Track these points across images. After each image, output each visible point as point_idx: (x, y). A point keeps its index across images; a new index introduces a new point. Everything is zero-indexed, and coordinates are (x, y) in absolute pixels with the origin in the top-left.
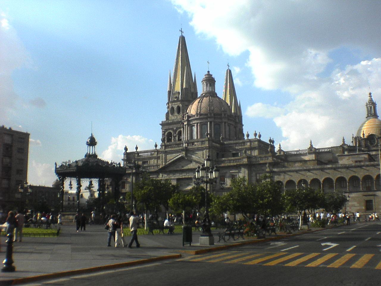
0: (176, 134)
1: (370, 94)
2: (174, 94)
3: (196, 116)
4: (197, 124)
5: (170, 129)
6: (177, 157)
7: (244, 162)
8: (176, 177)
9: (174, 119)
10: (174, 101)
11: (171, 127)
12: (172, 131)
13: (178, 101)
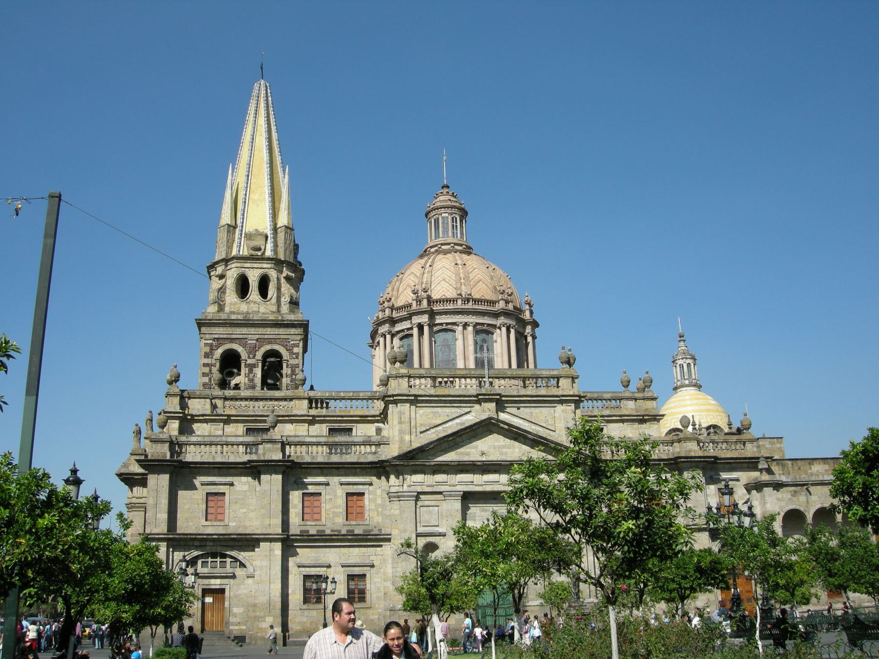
0: (254, 357)
2: (249, 236)
3: (460, 302)
4: (465, 325)
5: (232, 340)
6: (458, 421)
7: (690, 451)
8: (459, 488)
9: (248, 313)
10: (251, 258)
11: (238, 332)
13: (262, 259)
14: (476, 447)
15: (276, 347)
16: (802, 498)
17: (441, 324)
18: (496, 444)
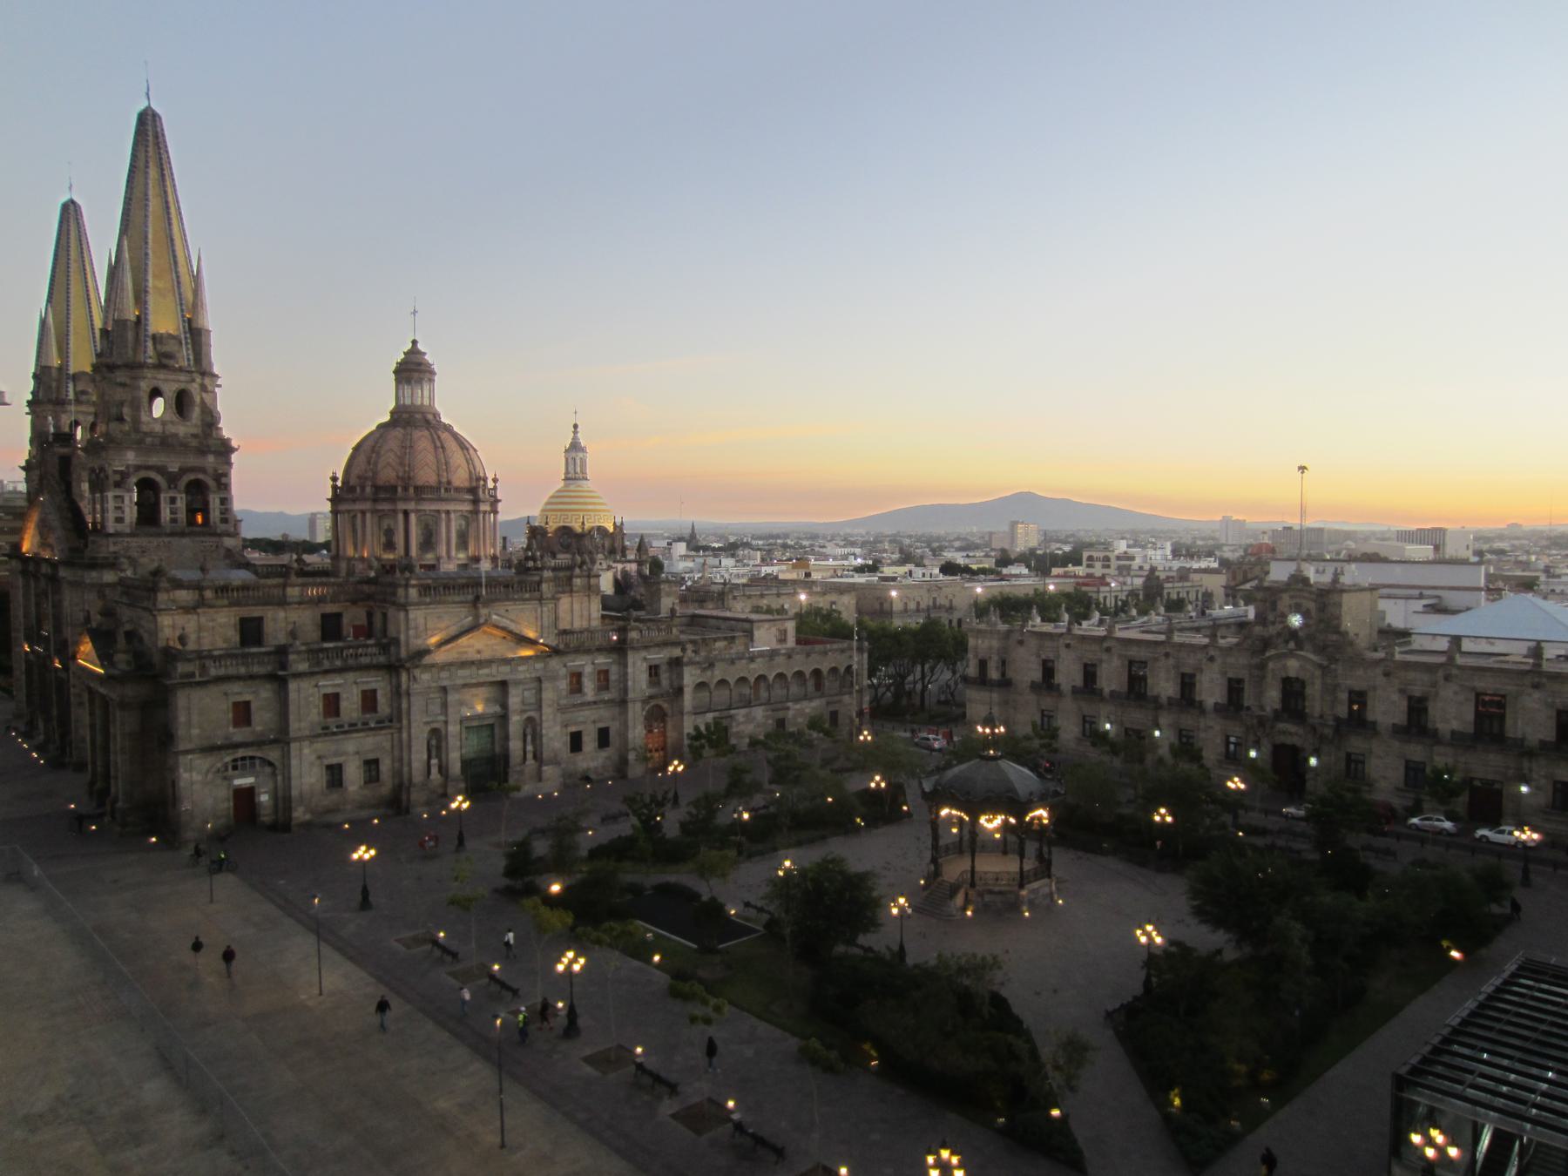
1: (576, 426)
4: (448, 512)
12: (158, 478)
15: (201, 476)
16: (709, 673)
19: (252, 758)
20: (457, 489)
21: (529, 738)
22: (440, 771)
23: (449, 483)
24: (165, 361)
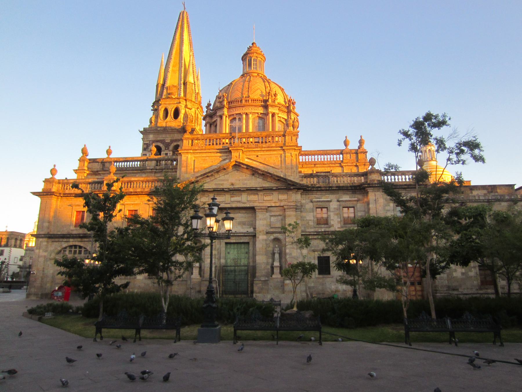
4: (247, 114)
5: (157, 141)
14: (228, 180)
17: (233, 115)
18: (241, 178)
19: (80, 247)
20: (254, 100)
21: (277, 256)
22: (200, 274)
23: (249, 97)
24: (170, 96)
